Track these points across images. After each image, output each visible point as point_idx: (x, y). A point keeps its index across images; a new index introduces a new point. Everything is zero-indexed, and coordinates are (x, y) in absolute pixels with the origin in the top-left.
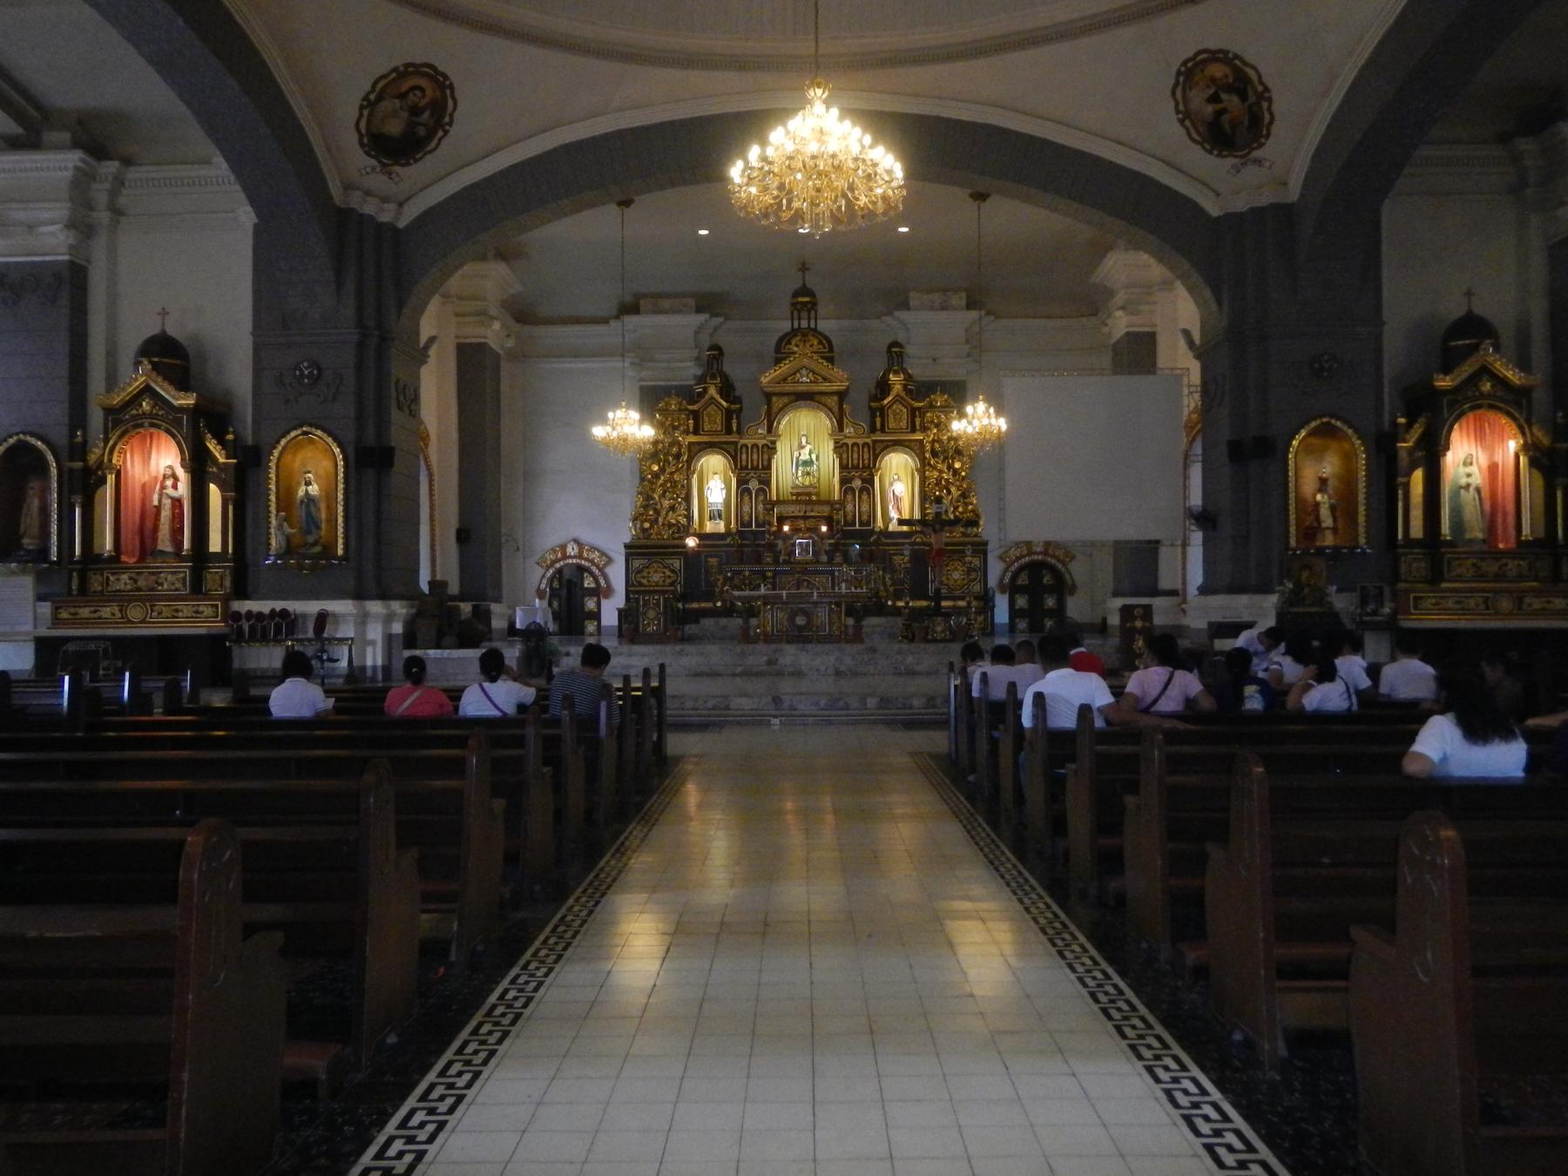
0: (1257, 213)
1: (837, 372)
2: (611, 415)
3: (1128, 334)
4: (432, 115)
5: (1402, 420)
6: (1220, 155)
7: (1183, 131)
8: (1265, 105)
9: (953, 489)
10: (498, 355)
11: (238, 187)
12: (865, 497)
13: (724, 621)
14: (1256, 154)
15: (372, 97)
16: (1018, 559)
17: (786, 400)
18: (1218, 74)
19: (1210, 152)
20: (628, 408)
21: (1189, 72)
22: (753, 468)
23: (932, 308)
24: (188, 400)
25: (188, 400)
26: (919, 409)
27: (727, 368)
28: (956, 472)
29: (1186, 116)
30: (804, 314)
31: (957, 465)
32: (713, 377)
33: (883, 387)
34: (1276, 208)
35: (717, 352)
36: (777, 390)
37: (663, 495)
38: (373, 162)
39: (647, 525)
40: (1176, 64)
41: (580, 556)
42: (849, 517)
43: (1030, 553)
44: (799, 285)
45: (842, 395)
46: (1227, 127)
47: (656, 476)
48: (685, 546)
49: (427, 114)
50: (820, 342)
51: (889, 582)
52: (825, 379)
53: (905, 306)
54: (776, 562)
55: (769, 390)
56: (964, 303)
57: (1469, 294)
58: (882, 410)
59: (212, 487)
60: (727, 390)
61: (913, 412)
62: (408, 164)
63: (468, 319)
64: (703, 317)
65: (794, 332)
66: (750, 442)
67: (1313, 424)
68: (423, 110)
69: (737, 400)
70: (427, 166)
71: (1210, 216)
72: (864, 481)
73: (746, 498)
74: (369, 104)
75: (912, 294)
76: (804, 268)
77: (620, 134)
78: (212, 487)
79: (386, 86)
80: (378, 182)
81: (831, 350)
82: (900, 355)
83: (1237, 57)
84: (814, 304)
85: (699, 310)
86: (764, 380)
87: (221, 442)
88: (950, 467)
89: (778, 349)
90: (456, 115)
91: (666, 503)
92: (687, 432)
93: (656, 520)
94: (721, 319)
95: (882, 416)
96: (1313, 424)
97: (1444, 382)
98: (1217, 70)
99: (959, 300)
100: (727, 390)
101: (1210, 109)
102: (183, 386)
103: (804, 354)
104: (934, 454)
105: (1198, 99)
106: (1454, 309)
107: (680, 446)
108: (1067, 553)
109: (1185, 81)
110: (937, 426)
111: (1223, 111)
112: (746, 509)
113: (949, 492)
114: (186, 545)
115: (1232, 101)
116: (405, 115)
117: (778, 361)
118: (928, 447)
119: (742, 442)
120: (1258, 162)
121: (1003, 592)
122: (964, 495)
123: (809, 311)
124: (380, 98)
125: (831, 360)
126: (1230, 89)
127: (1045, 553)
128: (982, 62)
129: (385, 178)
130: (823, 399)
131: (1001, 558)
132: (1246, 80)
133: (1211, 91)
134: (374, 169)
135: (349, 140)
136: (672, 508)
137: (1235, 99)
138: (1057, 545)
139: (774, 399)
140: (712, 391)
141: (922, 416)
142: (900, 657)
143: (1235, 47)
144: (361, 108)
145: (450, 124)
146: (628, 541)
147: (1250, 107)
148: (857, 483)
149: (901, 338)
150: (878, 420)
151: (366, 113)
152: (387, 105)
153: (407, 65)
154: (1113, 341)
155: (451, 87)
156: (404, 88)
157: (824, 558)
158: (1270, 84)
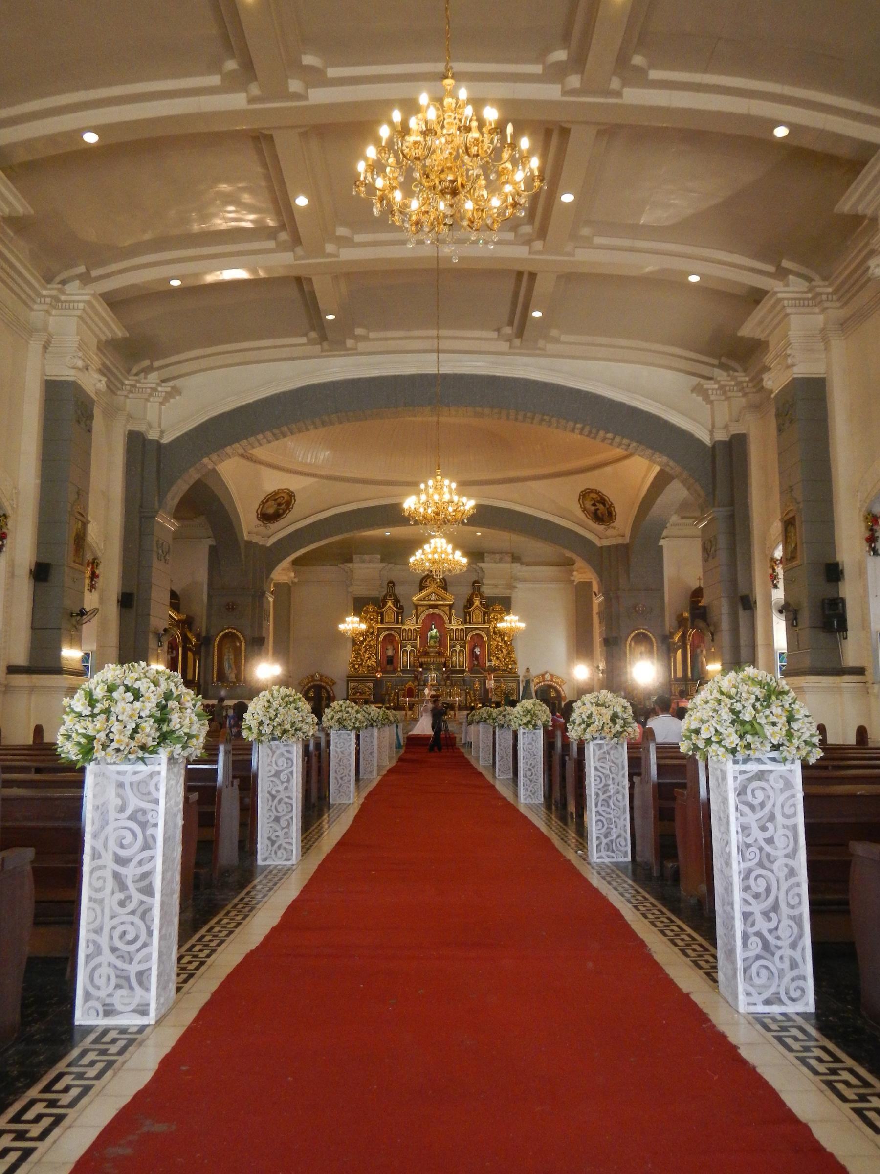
0: (617, 546)
1: (448, 596)
2: (347, 619)
17: (425, 608)
21: (584, 495)
23: (495, 562)
25: (183, 617)
26: (487, 613)
27: (397, 592)
28: (505, 642)
29: (584, 510)
31: (506, 639)
32: (390, 596)
33: (470, 602)
34: (623, 545)
35: (392, 584)
39: (357, 666)
41: (321, 680)
47: (362, 642)
48: (376, 677)
49: (283, 506)
58: (469, 613)
61: (485, 613)
64: (384, 565)
66: (407, 628)
67: (632, 635)
69: (401, 607)
70: (282, 522)
74: (263, 503)
80: (262, 529)
81: (446, 585)
82: (479, 588)
85: (382, 560)
86: (414, 599)
88: (503, 639)
89: (421, 585)
91: (367, 656)
92: (377, 622)
96: (632, 635)
98: (594, 496)
99: (508, 558)
100: (396, 602)
101: (593, 508)
104: (495, 633)
105: (588, 504)
106: (695, 585)
107: (373, 627)
108: (562, 681)
111: (598, 509)
115: (600, 506)
117: (421, 590)
120: (614, 528)
122: (509, 653)
124: (267, 501)
125: (446, 590)
126: (599, 502)
127: (551, 681)
128: (504, 486)
130: (442, 608)
132: (605, 500)
136: (369, 658)
138: (558, 678)
140: (390, 604)
143: (599, 489)
148: (458, 648)
152: (269, 503)
157: (443, 683)
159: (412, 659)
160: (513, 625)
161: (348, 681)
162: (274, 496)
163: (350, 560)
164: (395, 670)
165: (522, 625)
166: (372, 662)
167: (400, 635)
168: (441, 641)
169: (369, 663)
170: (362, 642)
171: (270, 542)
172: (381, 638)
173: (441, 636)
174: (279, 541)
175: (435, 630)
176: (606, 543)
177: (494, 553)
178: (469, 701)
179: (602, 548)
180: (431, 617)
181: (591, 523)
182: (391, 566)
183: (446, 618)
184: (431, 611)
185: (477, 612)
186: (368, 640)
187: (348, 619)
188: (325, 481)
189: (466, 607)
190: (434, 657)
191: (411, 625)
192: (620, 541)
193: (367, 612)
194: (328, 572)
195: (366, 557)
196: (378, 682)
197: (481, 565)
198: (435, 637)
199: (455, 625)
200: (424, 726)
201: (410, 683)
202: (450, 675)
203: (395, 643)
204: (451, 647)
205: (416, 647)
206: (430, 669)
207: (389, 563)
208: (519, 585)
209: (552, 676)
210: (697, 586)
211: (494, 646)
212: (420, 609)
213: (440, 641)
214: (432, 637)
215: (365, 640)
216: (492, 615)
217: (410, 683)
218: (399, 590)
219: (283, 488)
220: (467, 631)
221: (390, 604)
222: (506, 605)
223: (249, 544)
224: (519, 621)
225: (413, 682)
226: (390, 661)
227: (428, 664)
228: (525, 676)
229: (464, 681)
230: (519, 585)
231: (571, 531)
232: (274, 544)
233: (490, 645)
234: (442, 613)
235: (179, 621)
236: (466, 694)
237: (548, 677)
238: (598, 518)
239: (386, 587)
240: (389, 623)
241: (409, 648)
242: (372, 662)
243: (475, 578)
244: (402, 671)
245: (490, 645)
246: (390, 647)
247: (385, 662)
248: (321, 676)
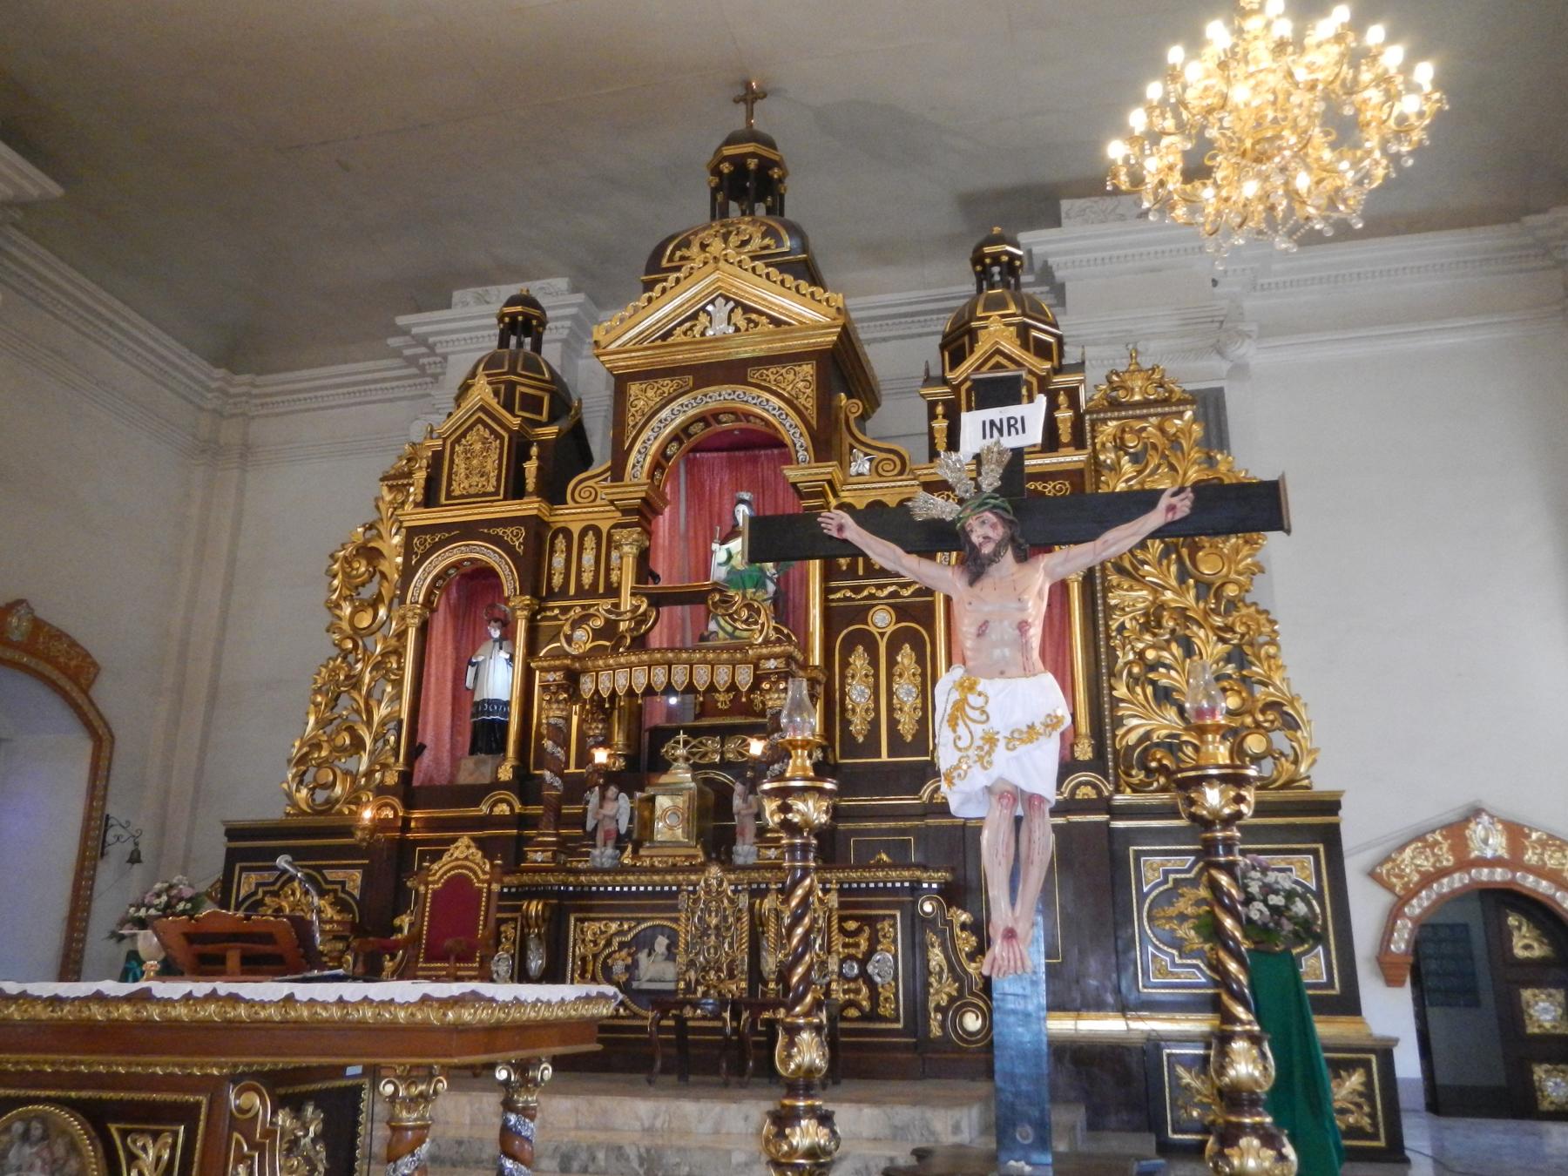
16: (1428, 879)
17: (668, 385)
22: (581, 593)
43: (1464, 864)
75: (1065, 205)
76: (749, 97)
113: (1188, 648)
121: (1392, 981)
122: (1238, 657)
127: (1514, 861)
130: (771, 373)
131: (1373, 875)
139: (634, 388)
161: (232, 856)
209: (1516, 832)
212: (641, 396)
237: (1489, 841)
240: (468, 498)
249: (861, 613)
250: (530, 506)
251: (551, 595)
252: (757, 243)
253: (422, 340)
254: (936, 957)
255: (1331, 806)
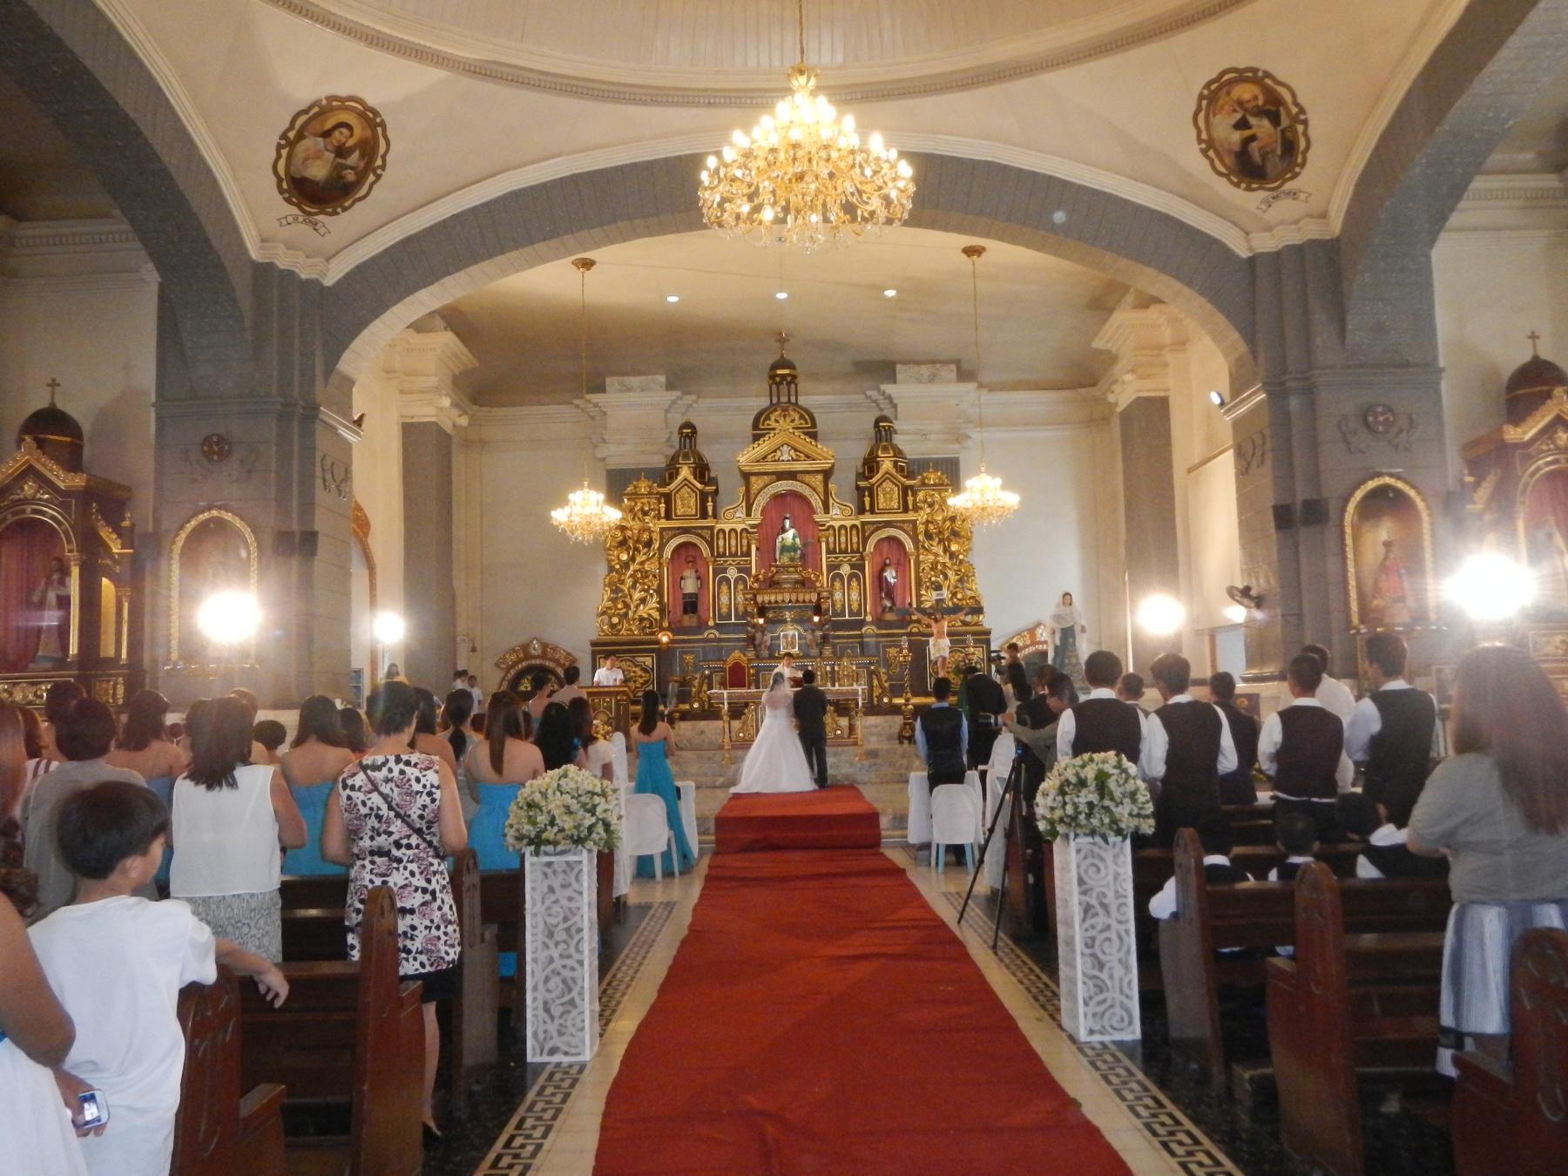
0: (1298, 252)
1: (821, 448)
3: (1138, 399)
4: (362, 156)
5: (1469, 479)
6: (1249, 189)
7: (1207, 162)
8: (1300, 128)
9: (950, 573)
10: (449, 437)
11: (139, 245)
12: (854, 584)
13: (703, 724)
14: (1288, 186)
15: (291, 135)
17: (766, 479)
18: (1246, 96)
19: (1237, 185)
20: (590, 487)
21: (1213, 95)
22: (731, 555)
24: (79, 481)
25: (79, 481)
26: (911, 487)
28: (952, 555)
29: (1209, 145)
30: (784, 387)
31: (954, 548)
32: (686, 456)
33: (871, 465)
35: (689, 432)
36: (756, 469)
37: (634, 586)
38: (295, 210)
39: (615, 620)
40: (1197, 87)
41: (544, 656)
42: (838, 606)
43: (1034, 643)
44: (777, 357)
45: (827, 474)
46: (1257, 158)
47: (626, 565)
48: (658, 642)
49: (354, 159)
50: (802, 417)
51: (884, 677)
52: (807, 456)
53: (892, 378)
54: (758, 657)
55: (747, 469)
56: (954, 375)
57: (1533, 337)
58: (871, 489)
59: (105, 581)
60: (702, 470)
61: (905, 490)
62: (335, 213)
63: (415, 397)
64: (675, 394)
65: (772, 407)
66: (727, 527)
68: (350, 151)
69: (713, 481)
71: (1238, 257)
72: (853, 566)
73: (724, 588)
74: (288, 142)
76: (782, 340)
77: (575, 180)
78: (105, 581)
79: (306, 124)
81: (814, 425)
82: (890, 431)
83: (1267, 75)
84: (794, 377)
85: (670, 386)
87: (118, 530)
88: (946, 550)
89: (756, 426)
90: (388, 158)
91: (637, 595)
93: (626, 614)
94: (694, 397)
95: (871, 495)
97: (1513, 434)
98: (1246, 92)
99: (950, 372)
100: (702, 470)
101: (1237, 136)
102: (73, 462)
103: (784, 427)
104: (929, 536)
107: (650, 532)
109: (1208, 106)
110: (931, 505)
111: (1253, 138)
112: (724, 599)
113: (946, 577)
114: (73, 649)
115: (1262, 126)
116: (330, 156)
117: (756, 438)
118: (921, 528)
119: (719, 526)
120: (1293, 194)
122: (961, 580)
123: (789, 384)
124: (300, 136)
125: (814, 436)
126: (1260, 112)
129: (308, 229)
130: (807, 478)
133: (1238, 116)
134: (296, 219)
135: (266, 186)
136: (643, 601)
137: (1266, 123)
139: (753, 479)
140: (685, 472)
141: (914, 495)
142: (904, 762)
143: (1264, 65)
144: (279, 147)
145: (383, 167)
146: (594, 638)
147: (1283, 131)
149: (888, 412)
150: (867, 500)
151: (284, 152)
152: (310, 143)
153: (330, 99)
154: (1120, 409)
155: (383, 125)
156: (329, 125)
157: (814, 651)
158: (1307, 107)
159: (740, 598)
160: (989, 496)
161: (594, 654)
162: (319, 121)
163: (601, 389)
164: (702, 626)
165: (1012, 499)
166: (650, 609)
167: (710, 544)
168: (807, 556)
169: (643, 611)
170: (626, 565)
171: (332, 275)
172: (668, 553)
173: (805, 545)
174: (361, 269)
175: (790, 535)
176: (1266, 243)
177: (918, 363)
178: (877, 692)
179: (1252, 261)
180: (778, 497)
181: (1224, 189)
182: (690, 398)
183: (816, 502)
184: (784, 486)
185: (888, 485)
186: (638, 559)
187: (576, 497)
188: (466, 82)
189: (861, 476)
190: (793, 590)
191: (734, 520)
192: (1311, 231)
193: (634, 496)
194: (552, 420)
195: (635, 381)
196: (664, 656)
197: (888, 388)
198: (793, 548)
199: (839, 516)
200: (773, 764)
201: (737, 654)
202: (833, 631)
203: (700, 563)
204: (831, 568)
205: (748, 571)
206: (784, 622)
207: (689, 393)
208: (975, 435)
210: (1524, 357)
211: (926, 566)
212: (756, 483)
213: (803, 557)
214: (784, 549)
215: (633, 559)
216: (921, 495)
217: (737, 654)
218: (708, 452)
219: (343, 93)
220: (864, 532)
221: (685, 472)
222: (951, 473)
223: (264, 272)
224: (1006, 486)
225: (743, 650)
226: (691, 605)
227: (778, 607)
228: (1057, 618)
229: (862, 645)
230: (975, 435)
231: (1165, 219)
232: (348, 277)
233: (918, 563)
234: (807, 492)
235: (67, 494)
236: (871, 674)
238: (1249, 168)
239: (676, 437)
241: (732, 574)
242: (650, 609)
243: (877, 414)
244: (717, 626)
245: (918, 563)
246: (689, 574)
247: (680, 609)
248: (545, 646)
249: (838, 567)
250: (708, 522)
251: (719, 555)
252: (797, 422)
253: (596, 405)
254: (875, 682)
255: (988, 633)
